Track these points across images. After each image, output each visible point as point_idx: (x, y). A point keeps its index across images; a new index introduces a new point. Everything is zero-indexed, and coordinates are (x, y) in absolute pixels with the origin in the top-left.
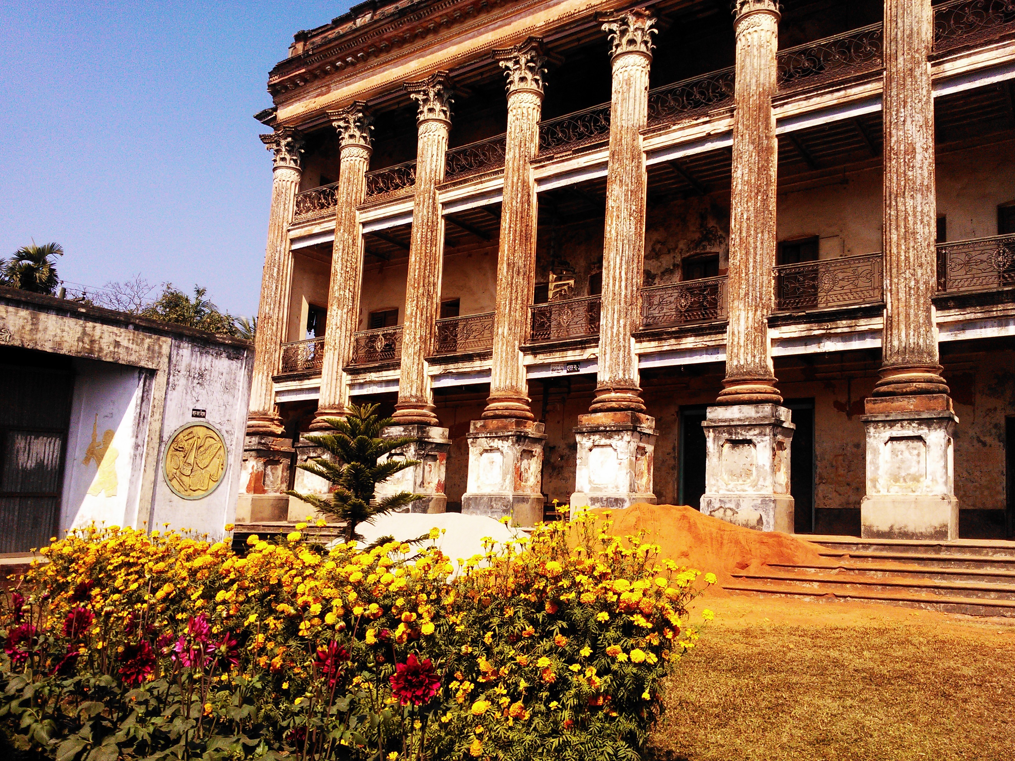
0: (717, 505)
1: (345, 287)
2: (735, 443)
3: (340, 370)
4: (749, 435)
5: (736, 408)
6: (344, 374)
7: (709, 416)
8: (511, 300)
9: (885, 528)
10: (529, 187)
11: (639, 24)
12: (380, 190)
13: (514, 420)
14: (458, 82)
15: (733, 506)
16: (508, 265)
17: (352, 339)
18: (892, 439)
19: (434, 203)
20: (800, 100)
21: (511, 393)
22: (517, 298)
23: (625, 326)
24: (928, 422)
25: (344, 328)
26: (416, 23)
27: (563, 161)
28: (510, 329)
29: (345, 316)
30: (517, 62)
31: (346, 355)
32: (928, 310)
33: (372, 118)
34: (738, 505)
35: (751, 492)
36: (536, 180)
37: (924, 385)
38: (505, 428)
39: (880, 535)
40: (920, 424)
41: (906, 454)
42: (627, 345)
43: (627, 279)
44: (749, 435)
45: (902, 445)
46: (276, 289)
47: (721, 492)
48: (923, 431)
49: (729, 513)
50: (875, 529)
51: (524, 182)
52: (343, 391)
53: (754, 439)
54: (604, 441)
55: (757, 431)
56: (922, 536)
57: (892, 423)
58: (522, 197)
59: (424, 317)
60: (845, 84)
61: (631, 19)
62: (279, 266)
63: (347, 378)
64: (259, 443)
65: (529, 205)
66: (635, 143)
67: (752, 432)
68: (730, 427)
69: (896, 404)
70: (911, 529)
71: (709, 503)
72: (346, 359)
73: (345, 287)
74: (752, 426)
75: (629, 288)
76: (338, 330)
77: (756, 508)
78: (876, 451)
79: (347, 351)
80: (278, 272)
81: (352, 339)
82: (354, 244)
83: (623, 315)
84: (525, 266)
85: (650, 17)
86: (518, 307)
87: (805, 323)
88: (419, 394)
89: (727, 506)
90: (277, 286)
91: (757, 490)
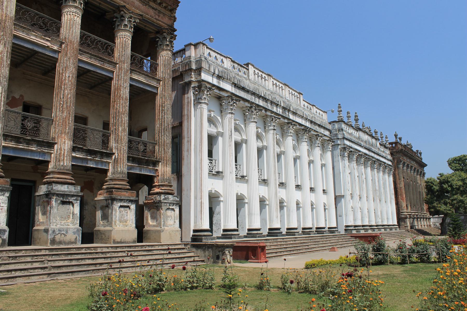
0: (57, 233)
2: (63, 203)
4: (71, 199)
5: (66, 186)
9: (119, 240)
15: (64, 233)
18: (121, 207)
24: (131, 201)
34: (67, 232)
35: (71, 226)
39: (118, 243)
41: (124, 212)
44: (71, 199)
45: (122, 209)
48: (129, 204)
49: (63, 236)
50: (116, 241)
53: (74, 202)
55: (75, 198)
56: (130, 242)
57: (121, 200)
67: (73, 198)
68: (63, 195)
69: (123, 193)
70: (127, 240)
74: (73, 196)
77: (74, 233)
78: (116, 210)
89: (62, 232)
91: (74, 225)
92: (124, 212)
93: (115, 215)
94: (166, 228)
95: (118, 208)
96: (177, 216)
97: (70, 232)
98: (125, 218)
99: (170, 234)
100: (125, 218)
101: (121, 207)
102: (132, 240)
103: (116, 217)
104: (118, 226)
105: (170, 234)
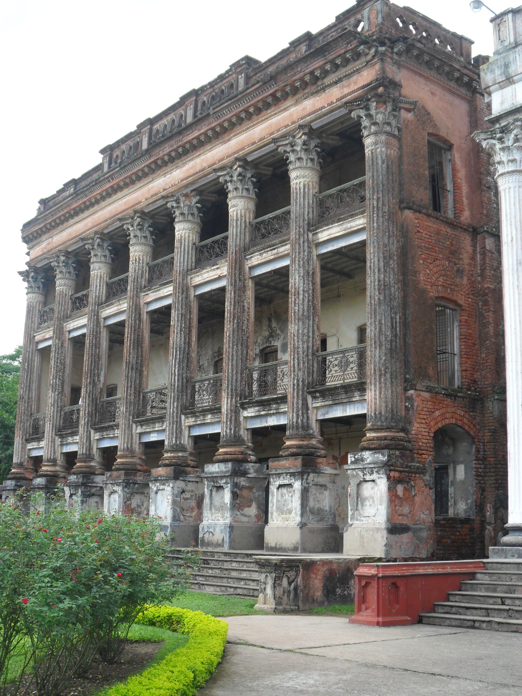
0: (206, 530)
1: (56, 377)
3: (54, 435)
6: (57, 438)
7: (206, 470)
8: (127, 388)
10: (140, 309)
11: (187, 202)
12: (78, 308)
13: (123, 472)
14: (113, 235)
16: (126, 363)
17: (62, 413)
19: (97, 319)
20: (257, 255)
21: (127, 453)
22: (131, 386)
23: (177, 407)
25: (56, 405)
26: (85, 199)
27: (156, 291)
28: (126, 408)
29: (56, 397)
30: (132, 226)
31: (58, 424)
32: (305, 400)
33: (74, 259)
34: (214, 530)
36: (145, 303)
37: (295, 450)
38: (118, 477)
40: (290, 476)
42: (178, 420)
43: (179, 374)
46: (27, 377)
47: (210, 521)
49: (211, 534)
51: (136, 306)
52: (56, 449)
54: (161, 487)
58: (135, 316)
59: (91, 398)
60: (273, 247)
61: (182, 199)
62: (28, 362)
63: (58, 441)
64: (16, 485)
65: (140, 321)
66: (185, 281)
69: (282, 463)
71: (203, 528)
72: (58, 427)
73: (56, 377)
75: (181, 381)
76: (52, 407)
79: (58, 421)
80: (28, 366)
81: (62, 413)
82: (62, 346)
83: (176, 399)
84: (137, 363)
85: (194, 196)
86: (132, 392)
87: (257, 406)
88: (88, 452)
90: (27, 376)
91: (224, 520)
92: (287, 495)
93: (272, 502)
94: (356, 522)
95: (275, 490)
96: (381, 497)
97: (218, 530)
98: (290, 506)
99: (362, 537)
100: (290, 506)
101: (280, 486)
102: (292, 546)
103: (273, 505)
104: (275, 521)
105: (362, 537)
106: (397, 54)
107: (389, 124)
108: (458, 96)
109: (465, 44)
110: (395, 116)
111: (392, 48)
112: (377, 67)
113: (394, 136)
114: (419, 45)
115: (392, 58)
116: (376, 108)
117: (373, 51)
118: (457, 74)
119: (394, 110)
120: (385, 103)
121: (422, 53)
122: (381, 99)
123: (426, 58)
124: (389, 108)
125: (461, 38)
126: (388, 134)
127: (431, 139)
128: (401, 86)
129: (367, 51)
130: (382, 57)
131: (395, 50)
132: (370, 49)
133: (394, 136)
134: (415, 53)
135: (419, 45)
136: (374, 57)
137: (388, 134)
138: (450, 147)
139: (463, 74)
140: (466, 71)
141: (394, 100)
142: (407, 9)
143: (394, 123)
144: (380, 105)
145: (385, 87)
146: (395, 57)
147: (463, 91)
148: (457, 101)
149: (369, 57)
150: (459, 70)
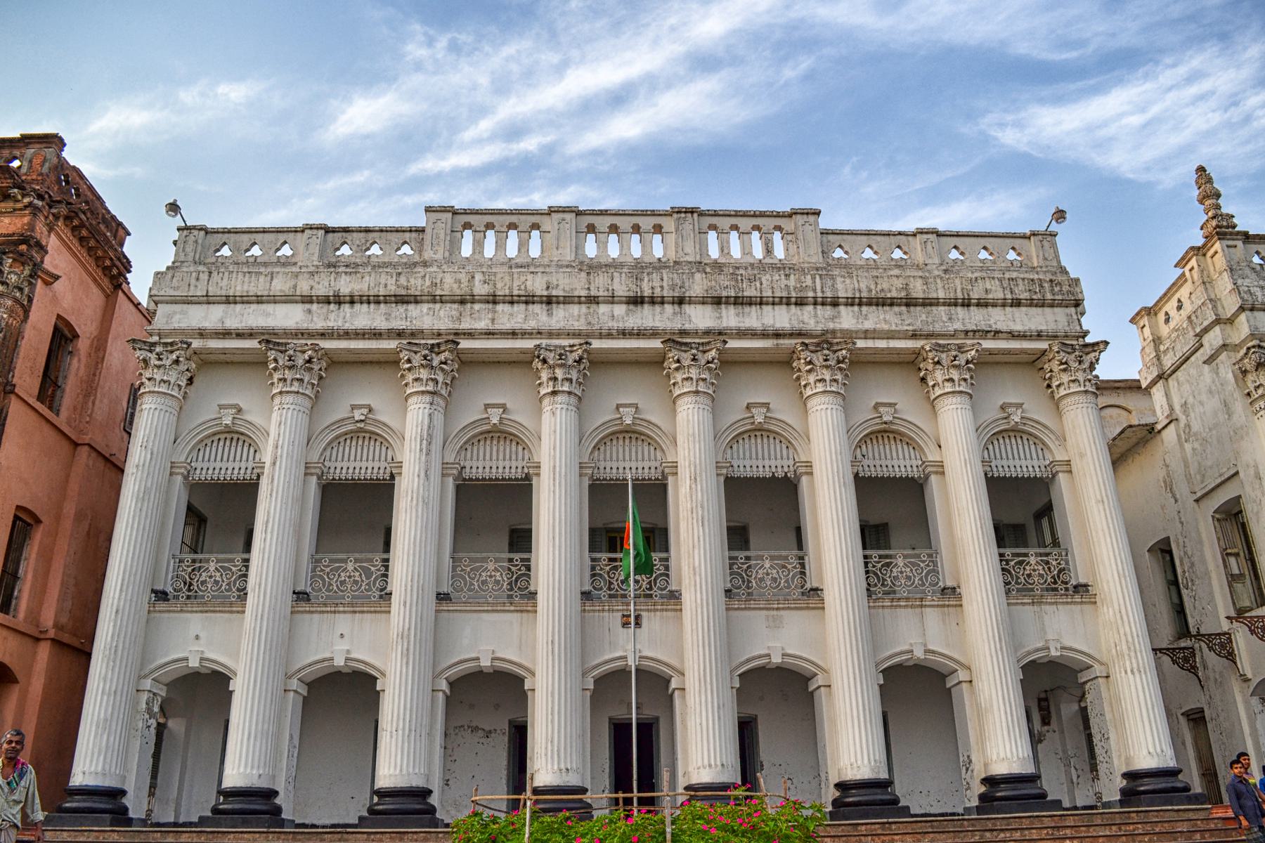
106: (54, 215)
107: (21, 290)
108: (99, 285)
109: (121, 232)
110: (30, 283)
111: (51, 207)
112: (26, 220)
113: (22, 306)
114: (83, 216)
115: (46, 218)
116: (11, 267)
117: (26, 200)
118: (108, 263)
119: (31, 276)
120: (23, 264)
121: (82, 225)
122: (21, 259)
123: (84, 233)
124: (27, 272)
125: (120, 224)
126: (16, 300)
127: (61, 325)
128: (47, 252)
129: (19, 197)
130: (35, 211)
131: (54, 211)
132: (24, 196)
133: (22, 306)
134: (76, 222)
135: (83, 216)
136: (26, 207)
137: (16, 300)
138: (76, 336)
139: (114, 265)
140: (118, 263)
141: (35, 265)
142: (75, 169)
143: (26, 290)
144: (17, 264)
145: (30, 246)
146: (51, 217)
147: (106, 283)
148: (95, 290)
149: (19, 205)
150: (111, 259)
